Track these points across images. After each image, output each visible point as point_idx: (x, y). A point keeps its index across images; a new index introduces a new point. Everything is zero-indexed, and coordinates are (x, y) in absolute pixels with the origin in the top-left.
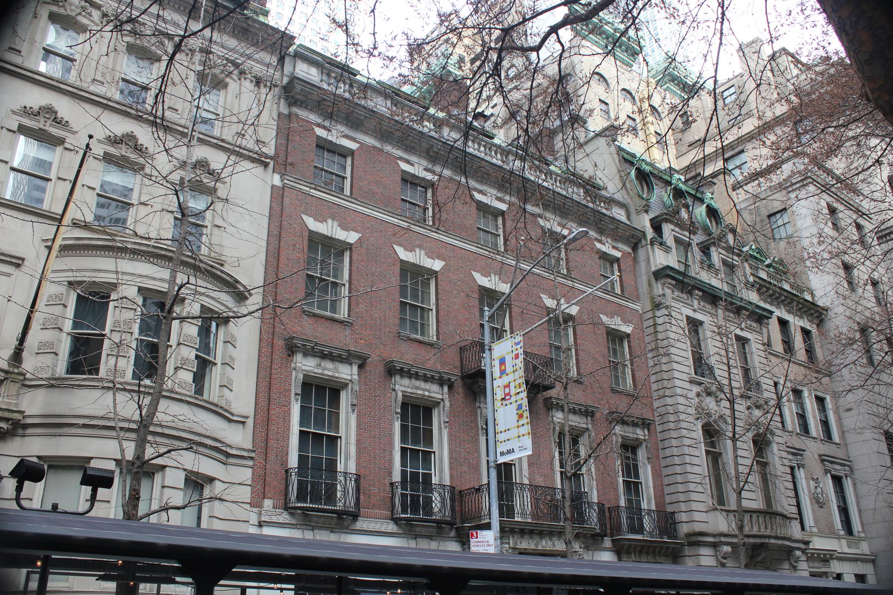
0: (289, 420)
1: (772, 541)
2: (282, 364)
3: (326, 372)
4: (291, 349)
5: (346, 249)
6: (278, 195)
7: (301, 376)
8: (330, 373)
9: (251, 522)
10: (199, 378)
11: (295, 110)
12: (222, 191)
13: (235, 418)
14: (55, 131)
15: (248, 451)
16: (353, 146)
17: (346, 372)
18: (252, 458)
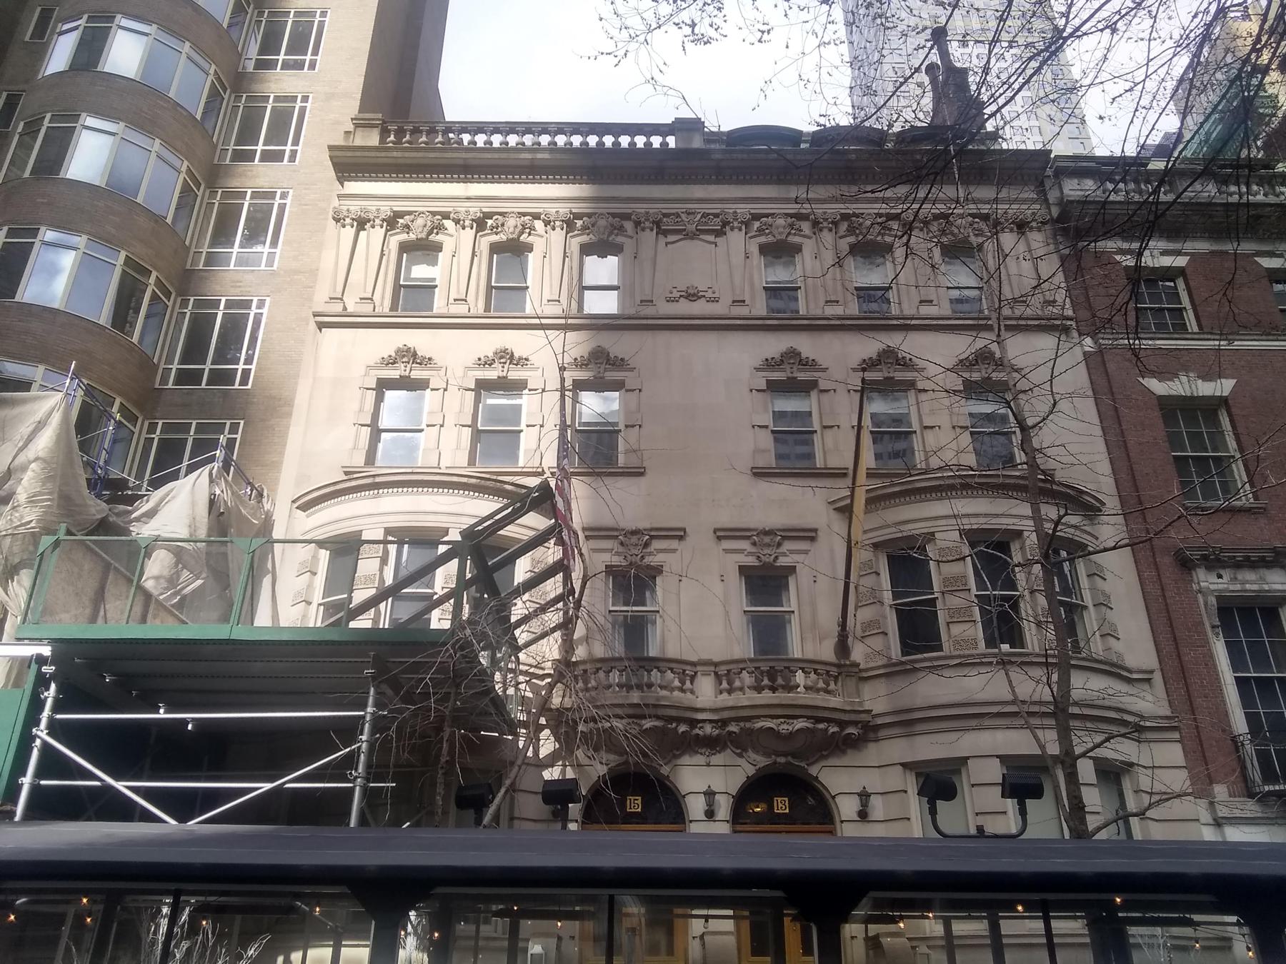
0: (1215, 666)
2: (1178, 589)
3: (1248, 586)
4: (1185, 565)
5: (1219, 406)
6: (1095, 362)
7: (1212, 600)
8: (1255, 587)
9: (1203, 821)
13: (1135, 676)
14: (802, 376)
15: (1167, 718)
16: (1181, 261)
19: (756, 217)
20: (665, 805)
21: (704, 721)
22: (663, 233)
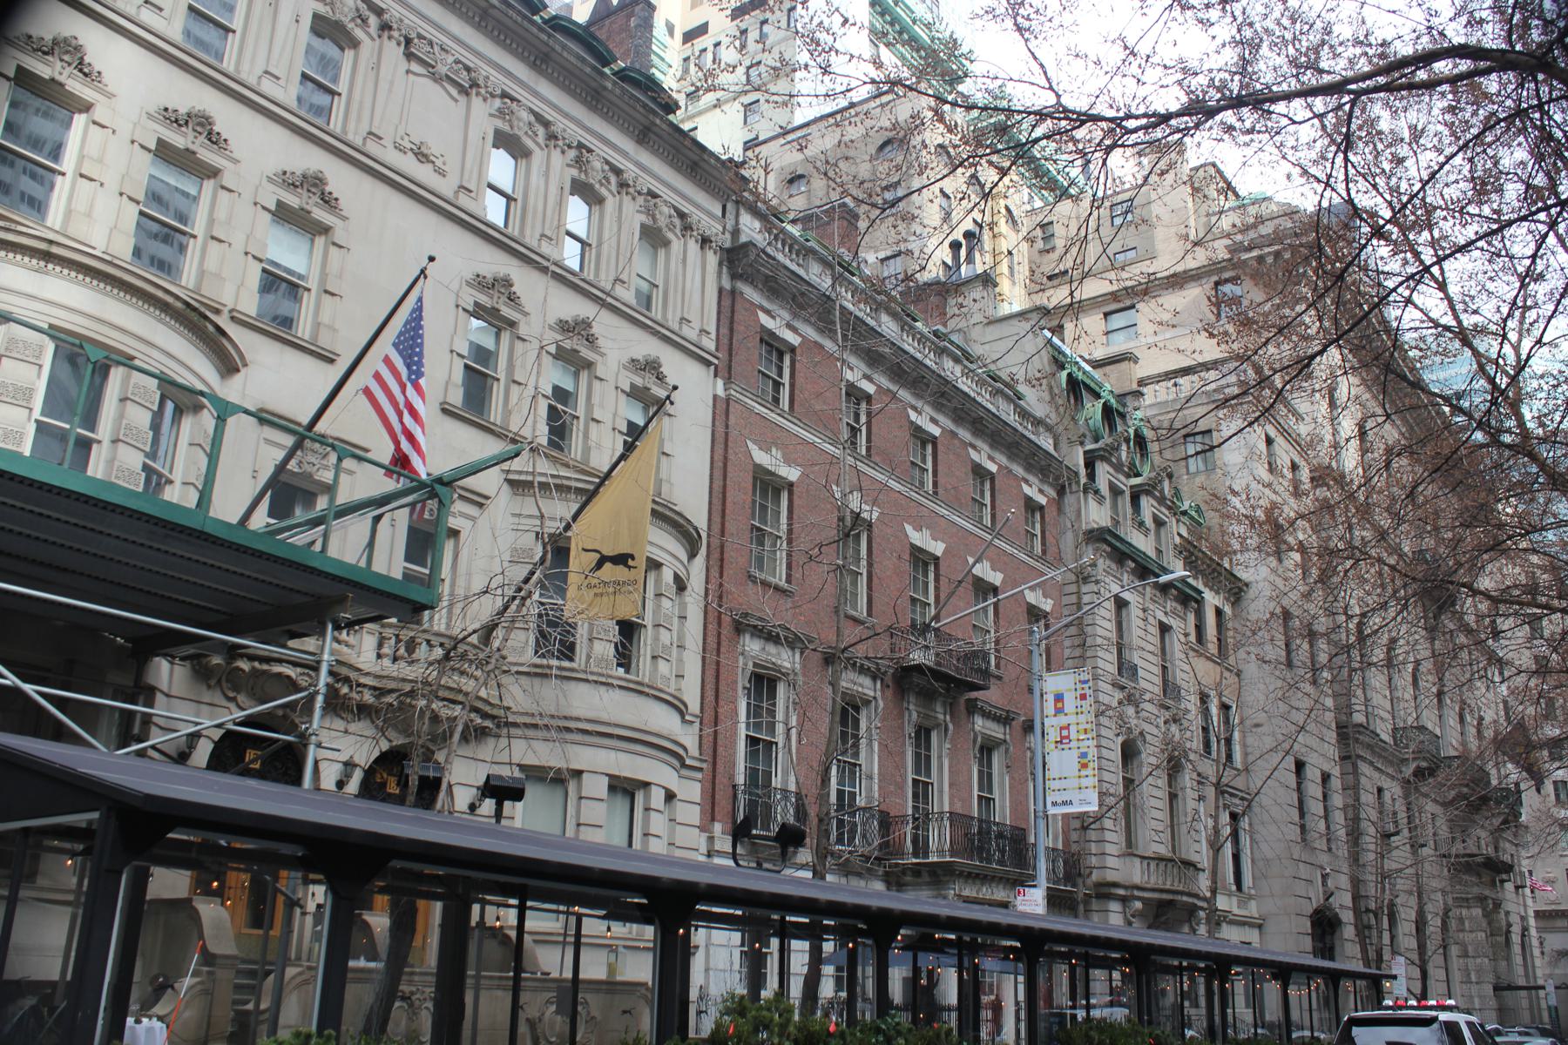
1: (1185, 898)
6: (722, 409)
10: (624, 658)
11: (740, 286)
12: (338, 236)
14: (506, 311)
17: (785, 659)
18: (700, 769)
19: (504, 95)
20: (286, 765)
21: (365, 686)
22: (409, 56)
